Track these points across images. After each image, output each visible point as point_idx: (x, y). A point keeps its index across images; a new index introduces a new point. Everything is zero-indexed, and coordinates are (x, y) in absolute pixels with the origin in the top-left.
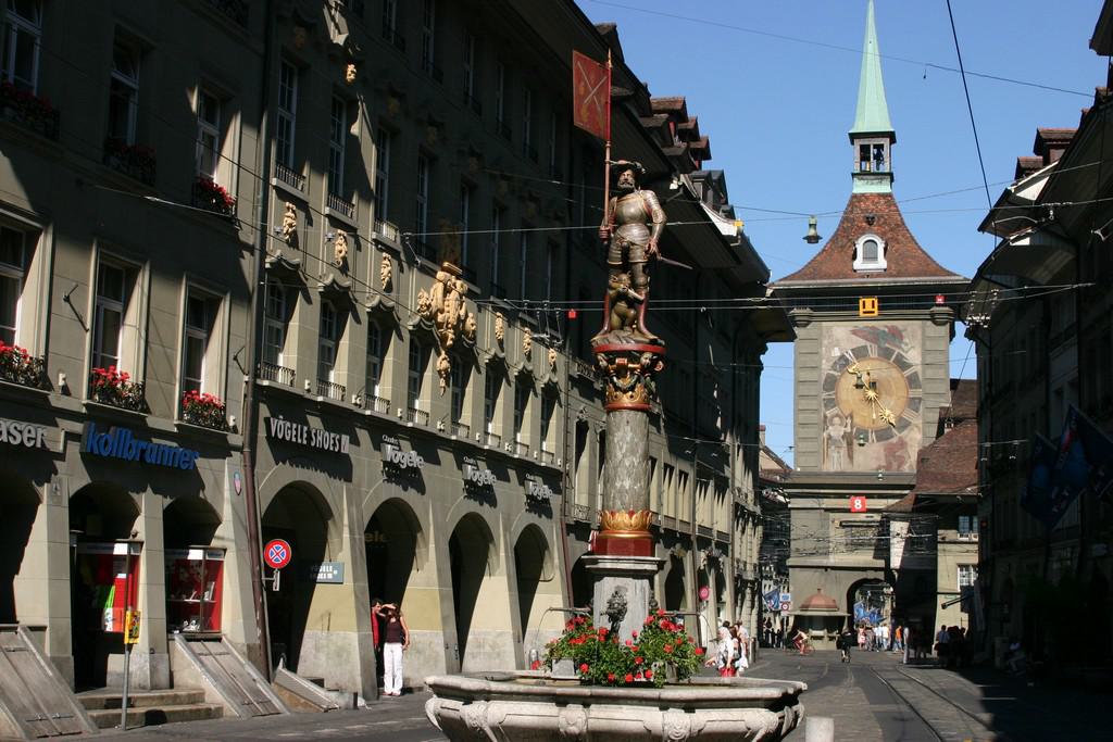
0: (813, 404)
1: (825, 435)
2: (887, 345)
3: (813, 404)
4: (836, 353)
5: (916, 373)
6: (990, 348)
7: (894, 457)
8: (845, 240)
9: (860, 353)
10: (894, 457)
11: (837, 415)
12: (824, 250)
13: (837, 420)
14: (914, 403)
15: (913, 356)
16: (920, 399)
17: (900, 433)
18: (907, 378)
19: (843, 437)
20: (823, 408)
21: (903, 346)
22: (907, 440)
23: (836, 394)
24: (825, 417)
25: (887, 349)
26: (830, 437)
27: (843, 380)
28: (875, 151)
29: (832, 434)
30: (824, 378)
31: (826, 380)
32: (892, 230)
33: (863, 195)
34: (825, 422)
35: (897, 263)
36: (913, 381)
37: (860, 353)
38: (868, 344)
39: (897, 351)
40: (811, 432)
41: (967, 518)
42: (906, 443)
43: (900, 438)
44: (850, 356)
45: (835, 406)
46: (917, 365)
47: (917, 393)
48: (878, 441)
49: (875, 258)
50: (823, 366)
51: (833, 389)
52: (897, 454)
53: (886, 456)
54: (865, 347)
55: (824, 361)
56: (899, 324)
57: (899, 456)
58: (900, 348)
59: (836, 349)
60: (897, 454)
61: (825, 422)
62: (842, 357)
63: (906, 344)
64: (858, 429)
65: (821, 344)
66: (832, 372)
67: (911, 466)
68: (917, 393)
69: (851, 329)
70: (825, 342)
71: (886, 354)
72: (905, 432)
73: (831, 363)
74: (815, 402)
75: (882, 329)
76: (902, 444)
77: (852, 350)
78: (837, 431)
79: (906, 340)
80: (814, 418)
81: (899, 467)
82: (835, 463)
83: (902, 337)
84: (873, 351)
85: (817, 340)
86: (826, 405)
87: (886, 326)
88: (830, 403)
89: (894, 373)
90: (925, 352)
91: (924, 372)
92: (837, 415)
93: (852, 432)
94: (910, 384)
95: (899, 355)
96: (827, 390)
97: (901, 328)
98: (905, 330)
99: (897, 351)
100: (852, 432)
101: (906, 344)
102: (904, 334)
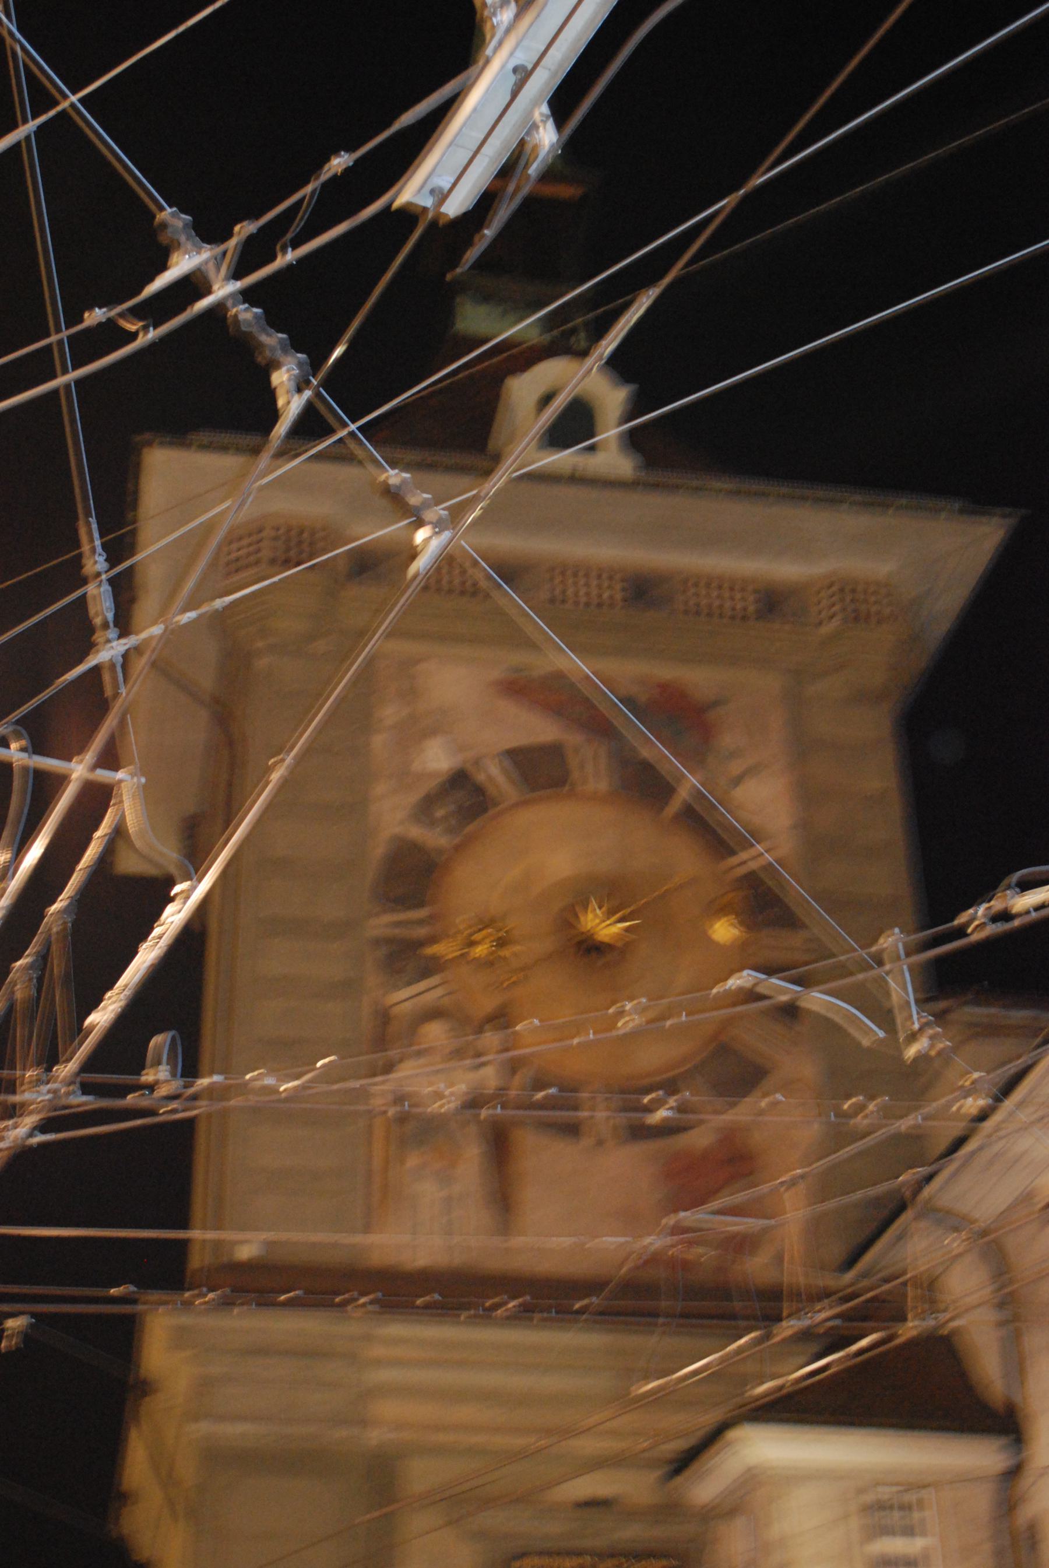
9: (541, 771)
30: (378, 851)
37: (541, 771)
44: (495, 775)
66: (416, 832)
71: (645, 786)
73: (413, 797)
78: (439, 1081)
79: (728, 740)
84: (593, 768)
89: (685, 859)
90: (808, 795)
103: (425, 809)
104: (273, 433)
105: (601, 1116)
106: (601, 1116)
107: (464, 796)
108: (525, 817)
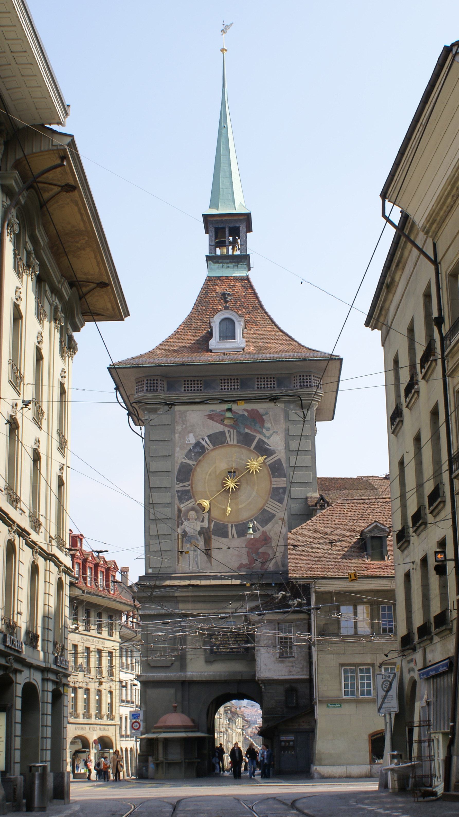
0: (164, 497)
1: (180, 531)
2: (247, 431)
3: (164, 497)
4: (191, 440)
5: (279, 460)
6: (435, 262)
7: (257, 553)
8: (199, 323)
9: (218, 440)
10: (257, 553)
11: (193, 509)
12: (177, 332)
13: (192, 514)
14: (277, 494)
15: (276, 442)
16: (284, 489)
17: (263, 527)
18: (269, 465)
19: (200, 533)
20: (177, 501)
21: (264, 431)
22: (272, 534)
23: (191, 485)
24: (180, 511)
25: (246, 433)
26: (185, 534)
27: (198, 469)
28: (231, 238)
29: (187, 530)
30: (177, 467)
31: (180, 471)
32: (249, 313)
33: (219, 278)
34: (179, 517)
35: (256, 343)
36: (276, 469)
37: (218, 440)
38: (226, 429)
39: (258, 436)
40: (163, 529)
41: (351, 608)
42: (270, 539)
43: (263, 531)
45: (191, 498)
46: (280, 451)
47: (281, 482)
48: (239, 536)
49: (233, 337)
50: (176, 455)
51: (188, 481)
52: (260, 550)
53: (248, 552)
54: (223, 433)
55: (177, 449)
56: (260, 407)
57: (263, 553)
58: (261, 433)
59: (191, 435)
60: (260, 550)
61: (179, 517)
62: (198, 444)
63: (268, 429)
64: (216, 524)
65: (174, 428)
66: (187, 461)
67: (276, 562)
68: (281, 482)
69: (208, 413)
70: (179, 428)
71: (246, 440)
72: (269, 526)
73: (186, 451)
74: (168, 494)
75: (241, 413)
76: (266, 539)
77: (209, 436)
78: (192, 526)
79: (268, 425)
80: (168, 512)
81: (263, 563)
82: (191, 564)
83: (262, 422)
84: (232, 438)
85: (171, 427)
86: (180, 498)
87: (246, 410)
88: (185, 495)
91: (288, 460)
92: (193, 509)
93: (209, 527)
94: (273, 473)
95: (261, 442)
96: (181, 481)
97: (261, 411)
98: (266, 414)
99: (258, 436)
100: (209, 527)
101: (268, 429)
102: (264, 417)
103: (188, 456)
104: (214, 231)
105: (232, 531)
106: (232, 531)
107: (199, 450)
108: (214, 454)
